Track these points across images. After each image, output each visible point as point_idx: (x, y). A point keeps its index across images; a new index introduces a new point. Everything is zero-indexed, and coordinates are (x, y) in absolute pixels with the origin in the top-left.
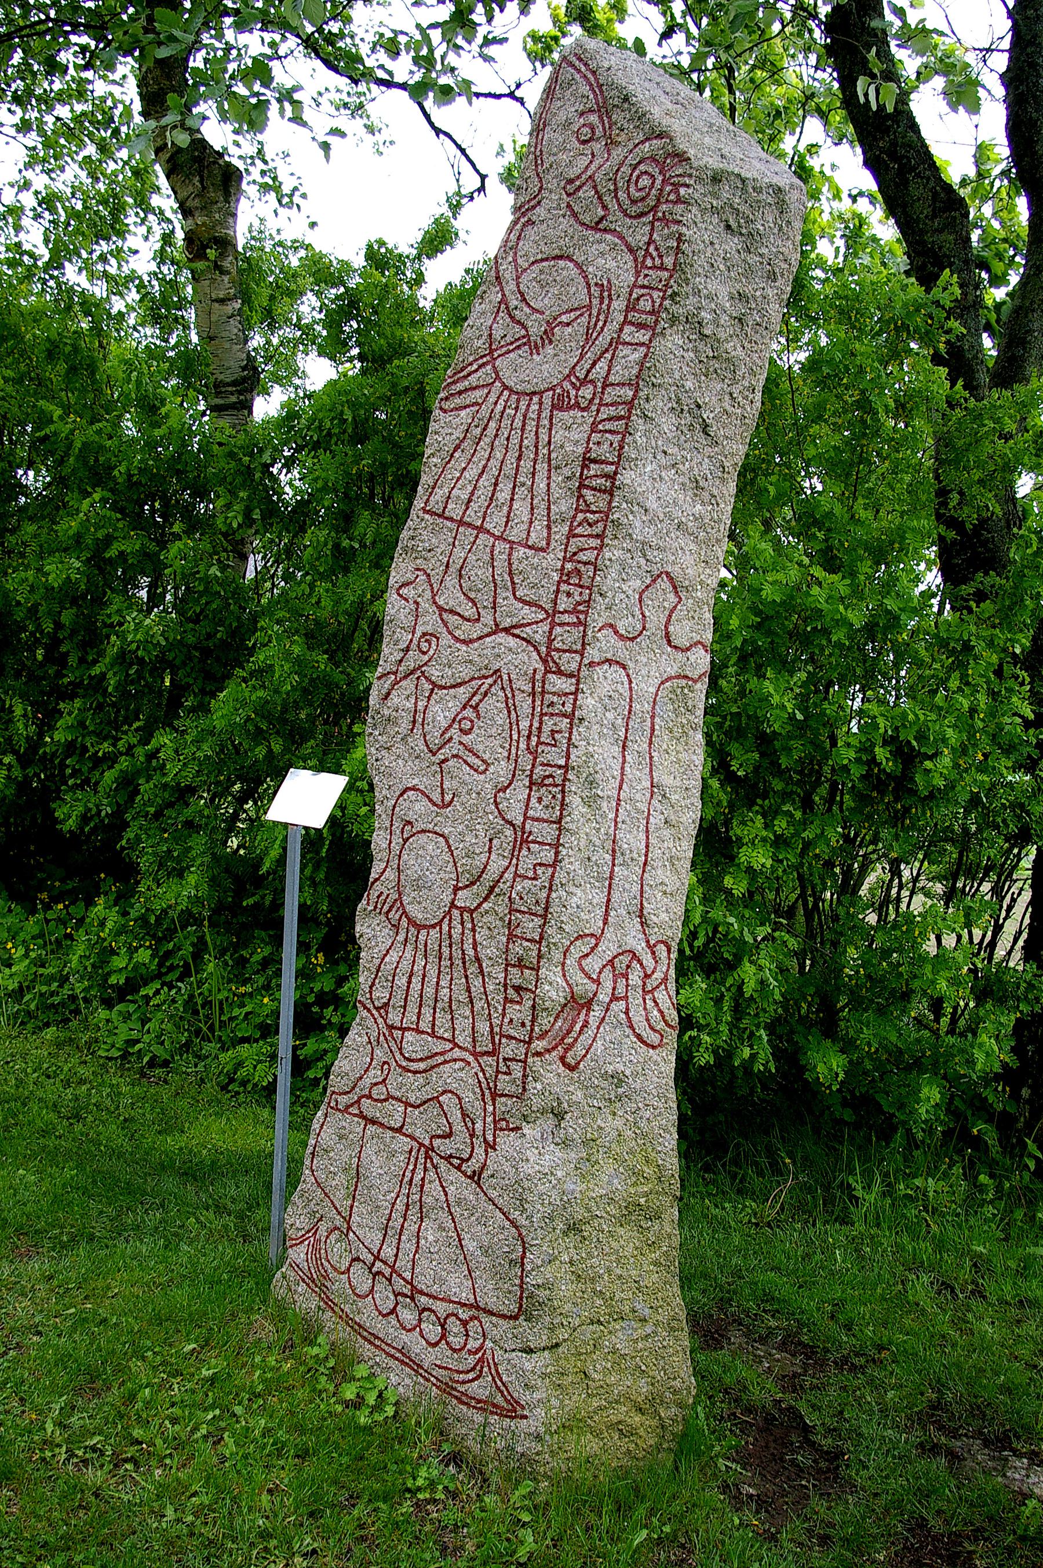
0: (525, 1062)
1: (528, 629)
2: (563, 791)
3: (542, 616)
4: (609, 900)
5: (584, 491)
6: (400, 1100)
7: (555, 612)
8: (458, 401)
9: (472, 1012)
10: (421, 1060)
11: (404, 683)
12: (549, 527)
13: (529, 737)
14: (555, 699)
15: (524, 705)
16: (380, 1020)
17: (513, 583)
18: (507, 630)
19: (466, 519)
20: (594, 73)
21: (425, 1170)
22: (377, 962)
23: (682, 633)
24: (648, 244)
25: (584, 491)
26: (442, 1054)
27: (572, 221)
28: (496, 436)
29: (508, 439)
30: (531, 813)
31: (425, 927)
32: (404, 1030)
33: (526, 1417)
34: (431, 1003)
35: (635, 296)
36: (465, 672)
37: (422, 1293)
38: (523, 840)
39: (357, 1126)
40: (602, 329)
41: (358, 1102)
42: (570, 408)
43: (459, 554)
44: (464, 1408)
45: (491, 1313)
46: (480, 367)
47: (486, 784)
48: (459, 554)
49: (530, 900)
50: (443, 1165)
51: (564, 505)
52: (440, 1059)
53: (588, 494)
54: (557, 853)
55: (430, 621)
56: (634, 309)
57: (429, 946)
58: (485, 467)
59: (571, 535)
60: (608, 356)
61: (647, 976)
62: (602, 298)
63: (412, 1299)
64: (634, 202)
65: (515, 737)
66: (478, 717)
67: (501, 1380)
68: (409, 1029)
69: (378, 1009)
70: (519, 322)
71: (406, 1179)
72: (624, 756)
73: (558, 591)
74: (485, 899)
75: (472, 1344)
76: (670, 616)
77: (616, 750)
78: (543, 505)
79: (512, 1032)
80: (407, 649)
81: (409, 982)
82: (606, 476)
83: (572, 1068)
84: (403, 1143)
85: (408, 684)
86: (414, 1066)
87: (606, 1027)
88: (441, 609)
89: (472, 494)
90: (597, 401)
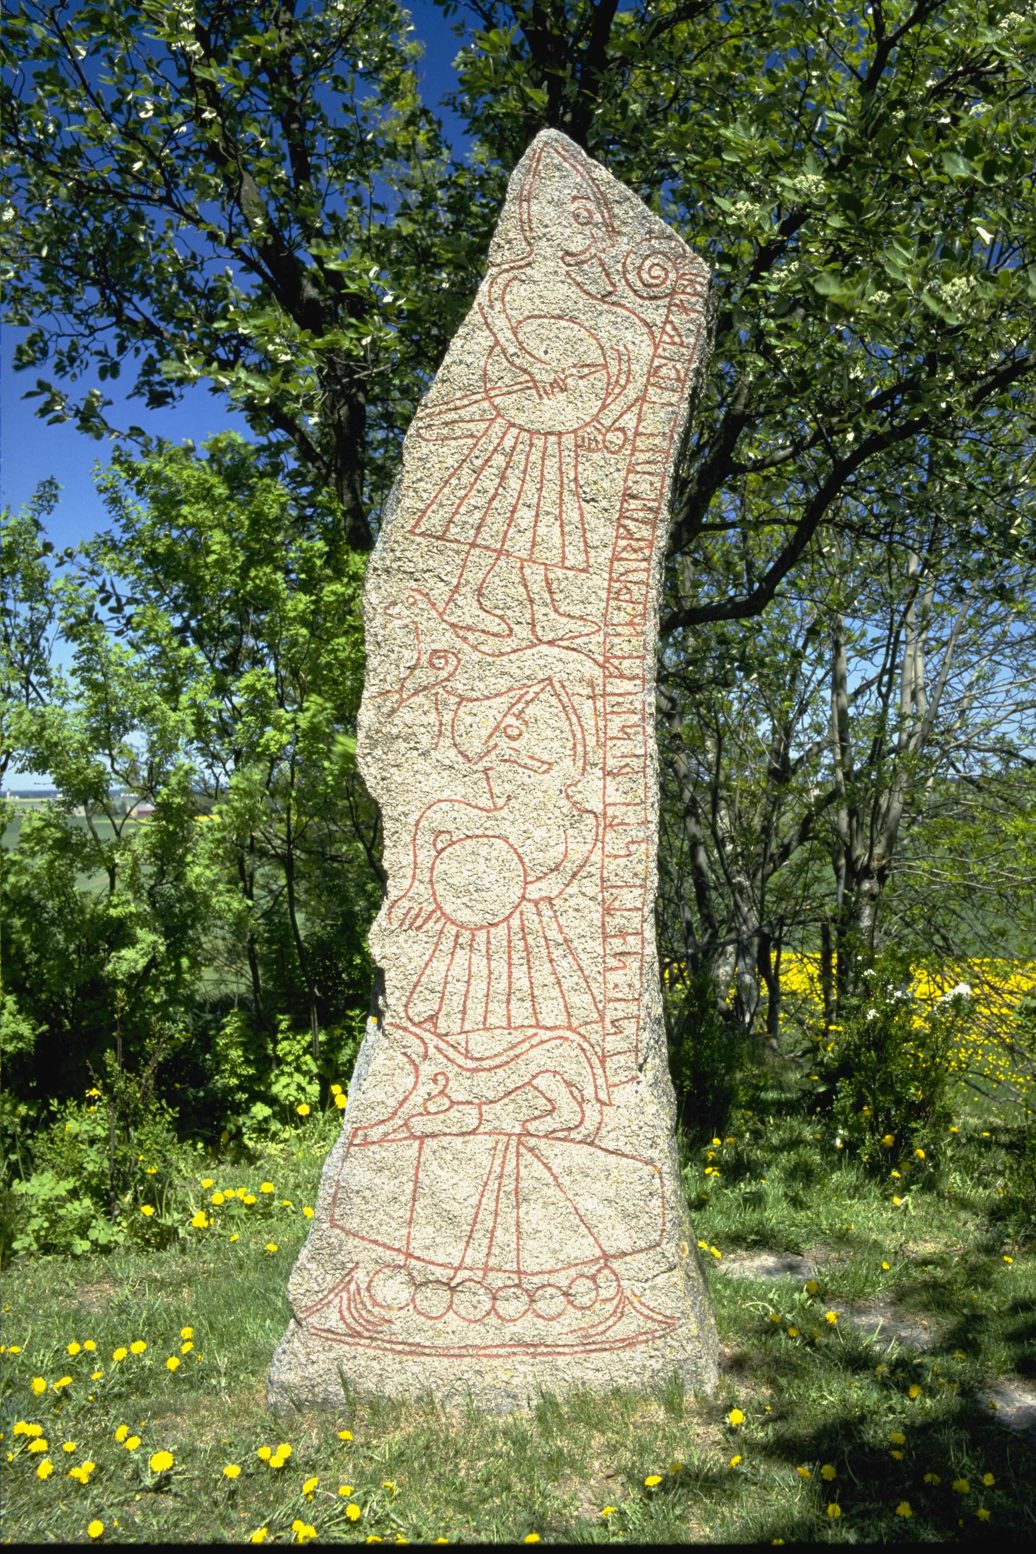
16: (426, 1036)
18: (551, 643)
21: (518, 1155)
48: (474, 577)
50: (543, 1144)
52: (526, 1046)
59: (615, 558)
69: (418, 1025)
86: (486, 1064)
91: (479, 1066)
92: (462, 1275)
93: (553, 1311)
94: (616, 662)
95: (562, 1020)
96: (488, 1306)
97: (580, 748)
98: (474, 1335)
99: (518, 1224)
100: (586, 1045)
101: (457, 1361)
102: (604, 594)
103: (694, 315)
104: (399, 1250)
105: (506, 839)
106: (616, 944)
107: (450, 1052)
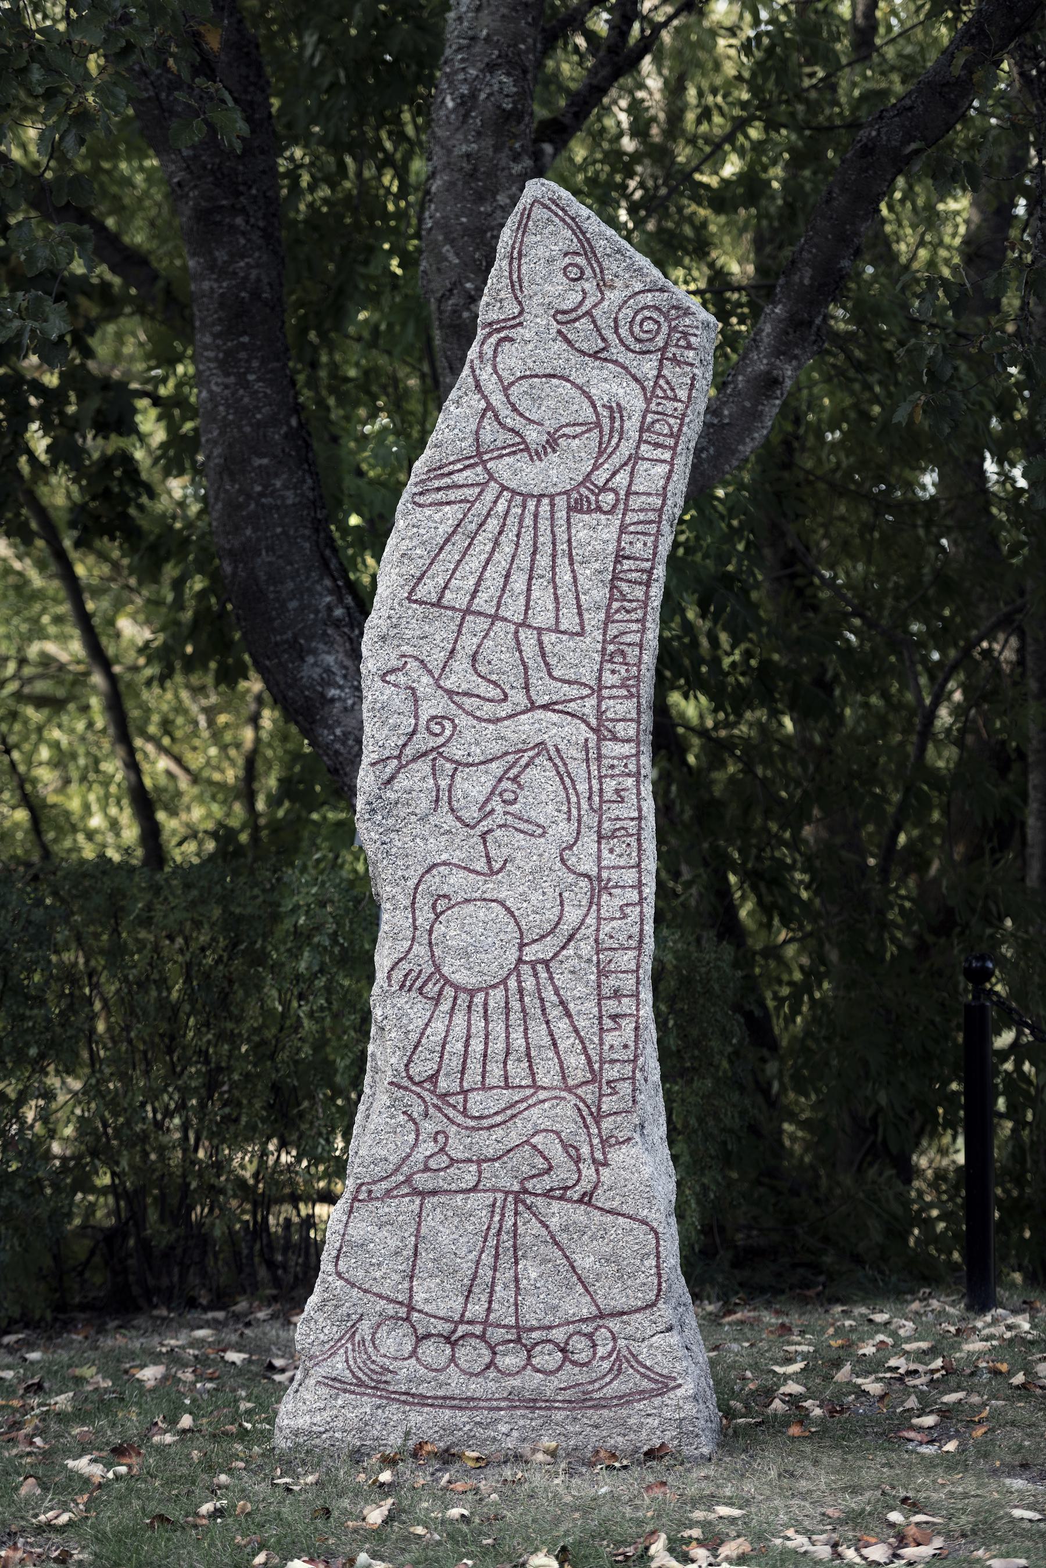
0: (633, 1078)
2: (639, 840)
3: (586, 692)
6: (470, 1161)
8: (440, 496)
9: (557, 1053)
10: (496, 1113)
12: (580, 614)
15: (578, 769)
16: (425, 1094)
17: (547, 664)
18: (544, 707)
19: (474, 608)
21: (516, 1214)
22: (414, 1037)
24: (658, 376)
26: (521, 1101)
27: (565, 346)
28: (500, 533)
30: (604, 863)
31: (480, 990)
34: (501, 1058)
35: (649, 419)
36: (496, 748)
37: (532, 1329)
38: (599, 886)
40: (618, 445)
42: (589, 511)
43: (469, 643)
44: (605, 1412)
45: (623, 1313)
48: (469, 643)
50: (540, 1202)
53: (624, 586)
54: (640, 893)
56: (648, 430)
57: (492, 1003)
59: (608, 620)
60: (628, 468)
62: (612, 419)
63: (518, 1340)
64: (639, 341)
65: (574, 799)
66: (521, 787)
68: (472, 1090)
69: (419, 1084)
70: (512, 430)
71: (493, 1231)
73: (600, 670)
74: (563, 948)
78: (571, 595)
79: (615, 1056)
80: (414, 732)
81: (467, 1045)
85: (423, 767)
86: (485, 1123)
88: (450, 693)
89: (478, 584)
91: (481, 1123)
92: (462, 1329)
93: (552, 1366)
94: (610, 725)
95: (557, 1081)
96: (487, 1360)
97: (574, 812)
98: (475, 1387)
99: (517, 1280)
100: (581, 1105)
101: (459, 1413)
102: (597, 657)
103: (688, 369)
104: (401, 1303)
105: (502, 904)
106: (611, 1006)
107: (451, 1112)
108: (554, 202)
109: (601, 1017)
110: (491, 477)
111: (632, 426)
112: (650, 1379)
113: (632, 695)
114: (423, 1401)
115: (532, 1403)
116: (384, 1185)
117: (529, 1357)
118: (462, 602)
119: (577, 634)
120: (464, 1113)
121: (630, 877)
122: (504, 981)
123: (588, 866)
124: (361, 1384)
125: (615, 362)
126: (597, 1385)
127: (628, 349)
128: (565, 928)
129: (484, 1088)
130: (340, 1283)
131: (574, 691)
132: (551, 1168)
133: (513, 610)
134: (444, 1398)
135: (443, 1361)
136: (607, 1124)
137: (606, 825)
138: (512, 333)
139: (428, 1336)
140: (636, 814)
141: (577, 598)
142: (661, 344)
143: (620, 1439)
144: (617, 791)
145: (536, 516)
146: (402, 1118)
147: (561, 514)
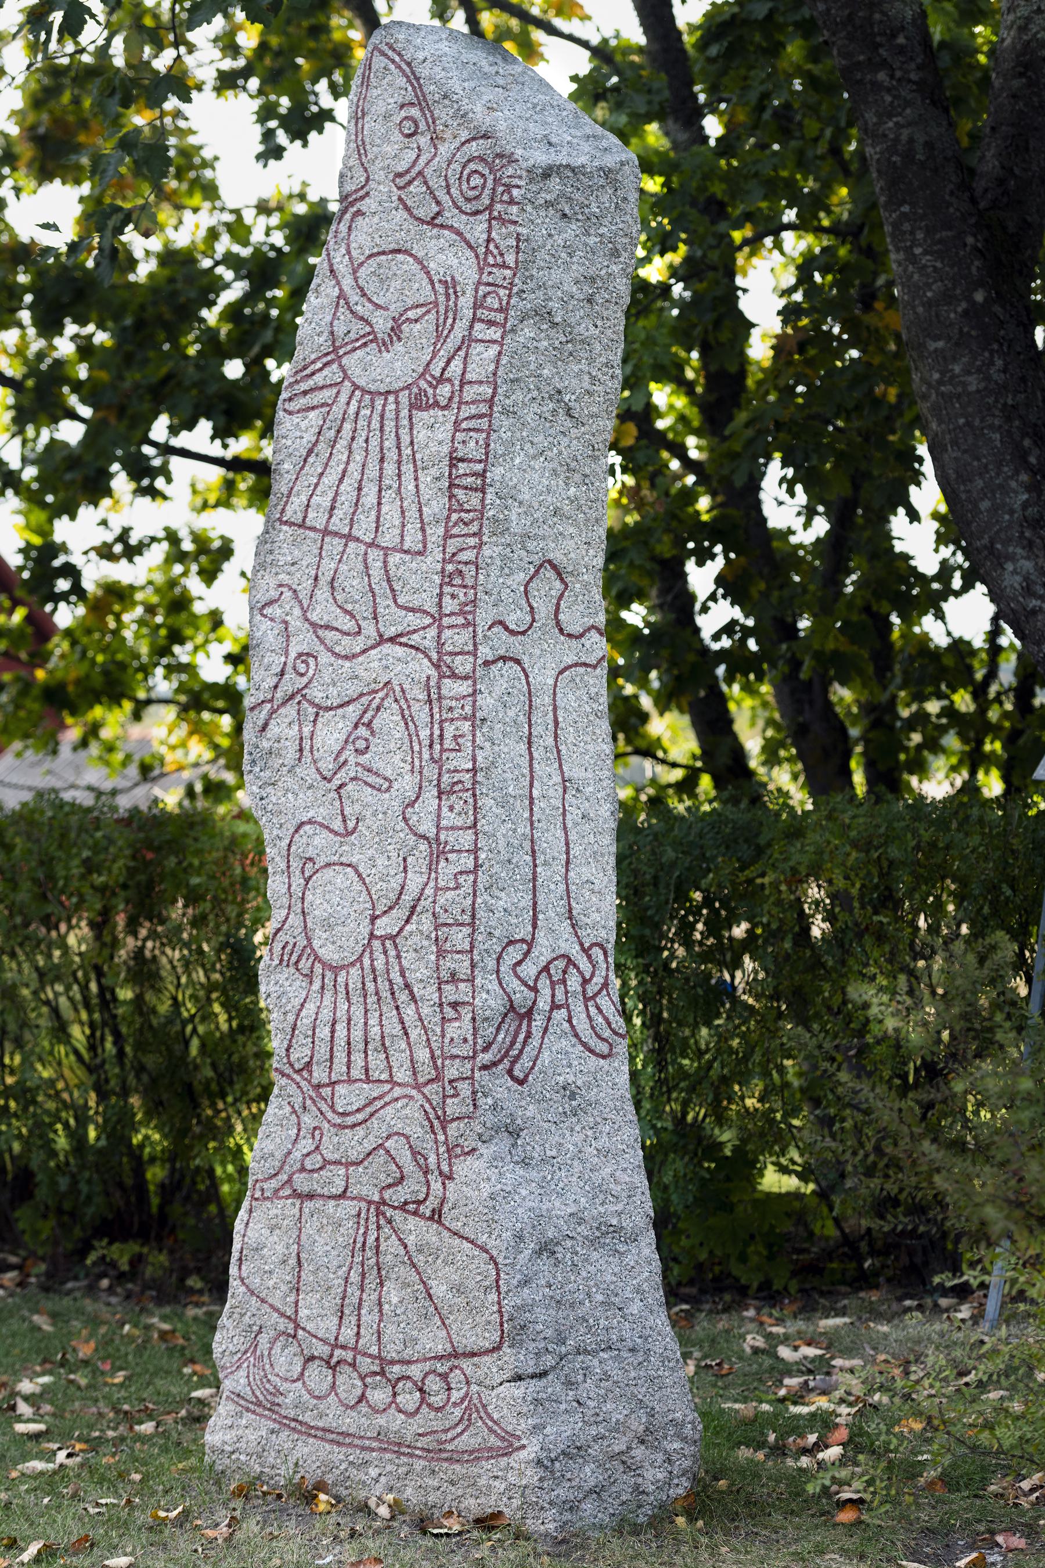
0: (472, 1078)
1: (415, 636)
3: (428, 621)
4: (535, 904)
5: (456, 491)
6: (340, 1163)
7: (442, 615)
8: (303, 401)
11: (282, 711)
12: (423, 530)
13: (431, 746)
14: (453, 703)
15: (422, 715)
16: (303, 1084)
17: (393, 590)
18: (392, 640)
19: (331, 528)
20: (409, 64)
21: (379, 1227)
22: (291, 1018)
23: (573, 619)
24: (489, 240)
25: (456, 491)
27: (406, 215)
28: (353, 439)
29: (367, 441)
31: (343, 967)
32: (333, 1084)
33: (524, 1447)
34: (362, 1046)
36: (352, 689)
37: (393, 1362)
38: (439, 852)
39: (290, 1208)
41: (289, 1181)
42: (429, 407)
43: (328, 566)
44: (457, 1467)
45: (473, 1354)
46: (325, 365)
47: (392, 802)
48: (328, 566)
49: (456, 911)
50: (398, 1216)
51: (436, 506)
52: (379, 1104)
54: (476, 858)
55: (303, 641)
56: (481, 306)
57: (351, 986)
58: (344, 471)
59: (447, 536)
61: (585, 982)
62: (447, 295)
63: (382, 1373)
64: (468, 200)
65: (416, 748)
66: (373, 733)
67: (492, 1419)
69: (299, 1072)
70: (362, 318)
72: (531, 753)
73: (440, 595)
74: (407, 921)
75: (456, 1396)
76: (558, 605)
77: (523, 747)
78: (414, 508)
79: (455, 1051)
80: (282, 673)
81: (333, 1032)
82: (474, 474)
83: (521, 1082)
84: (349, 1207)
85: (290, 711)
86: (350, 1120)
87: (550, 1037)
88: (313, 625)
89: (334, 500)
90: (456, 399)
94: (448, 659)
96: (359, 1392)
98: (349, 1422)
99: (380, 1304)
101: (336, 1449)
102: (437, 579)
103: (512, 228)
107: (324, 1108)
108: (391, 47)
109: (441, 1005)
110: (346, 376)
111: (466, 302)
112: (497, 1435)
113: (468, 624)
114: (309, 1431)
115: (398, 1447)
116: (274, 1184)
117: (395, 1395)
118: (320, 524)
119: (419, 553)
120: (332, 1107)
121: (466, 839)
122: (360, 959)
123: (427, 827)
124: (259, 1404)
125: (450, 228)
126: (450, 1435)
127: (462, 212)
128: (407, 899)
129: (350, 1081)
130: (243, 1289)
131: (415, 620)
132: (402, 1178)
133: (364, 528)
134: (324, 1430)
135: (326, 1386)
136: (453, 1129)
137: (445, 778)
138: (362, 205)
139: (312, 1358)
140: (470, 766)
141: (420, 510)
142: (487, 202)
143: (472, 1501)
144: (455, 737)
145: (382, 416)
146: (288, 1109)
147: (404, 413)
